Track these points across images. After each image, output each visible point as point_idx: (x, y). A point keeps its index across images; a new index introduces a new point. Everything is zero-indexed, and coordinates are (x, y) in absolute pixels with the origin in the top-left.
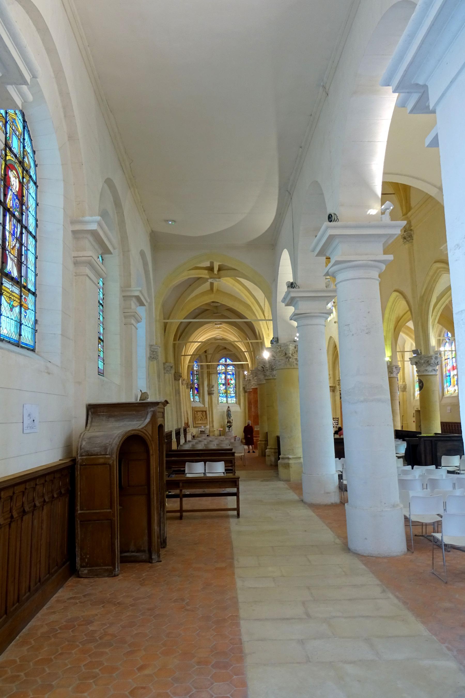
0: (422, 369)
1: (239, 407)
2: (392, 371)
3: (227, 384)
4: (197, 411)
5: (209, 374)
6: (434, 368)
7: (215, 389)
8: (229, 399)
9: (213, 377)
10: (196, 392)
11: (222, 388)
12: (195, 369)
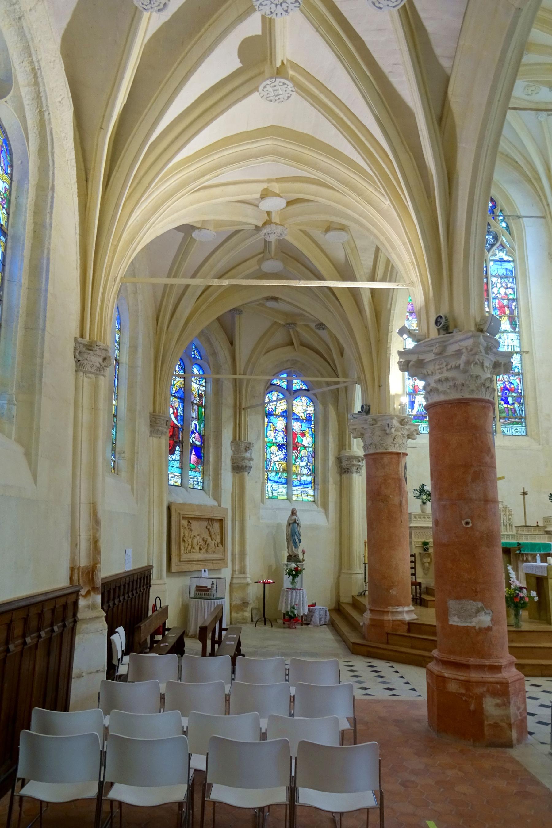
1: (325, 517)
3: (289, 445)
4: (190, 519)
5: (238, 411)
7: (255, 453)
8: (296, 491)
9: (251, 420)
10: (193, 457)
11: (277, 456)
12: (194, 386)
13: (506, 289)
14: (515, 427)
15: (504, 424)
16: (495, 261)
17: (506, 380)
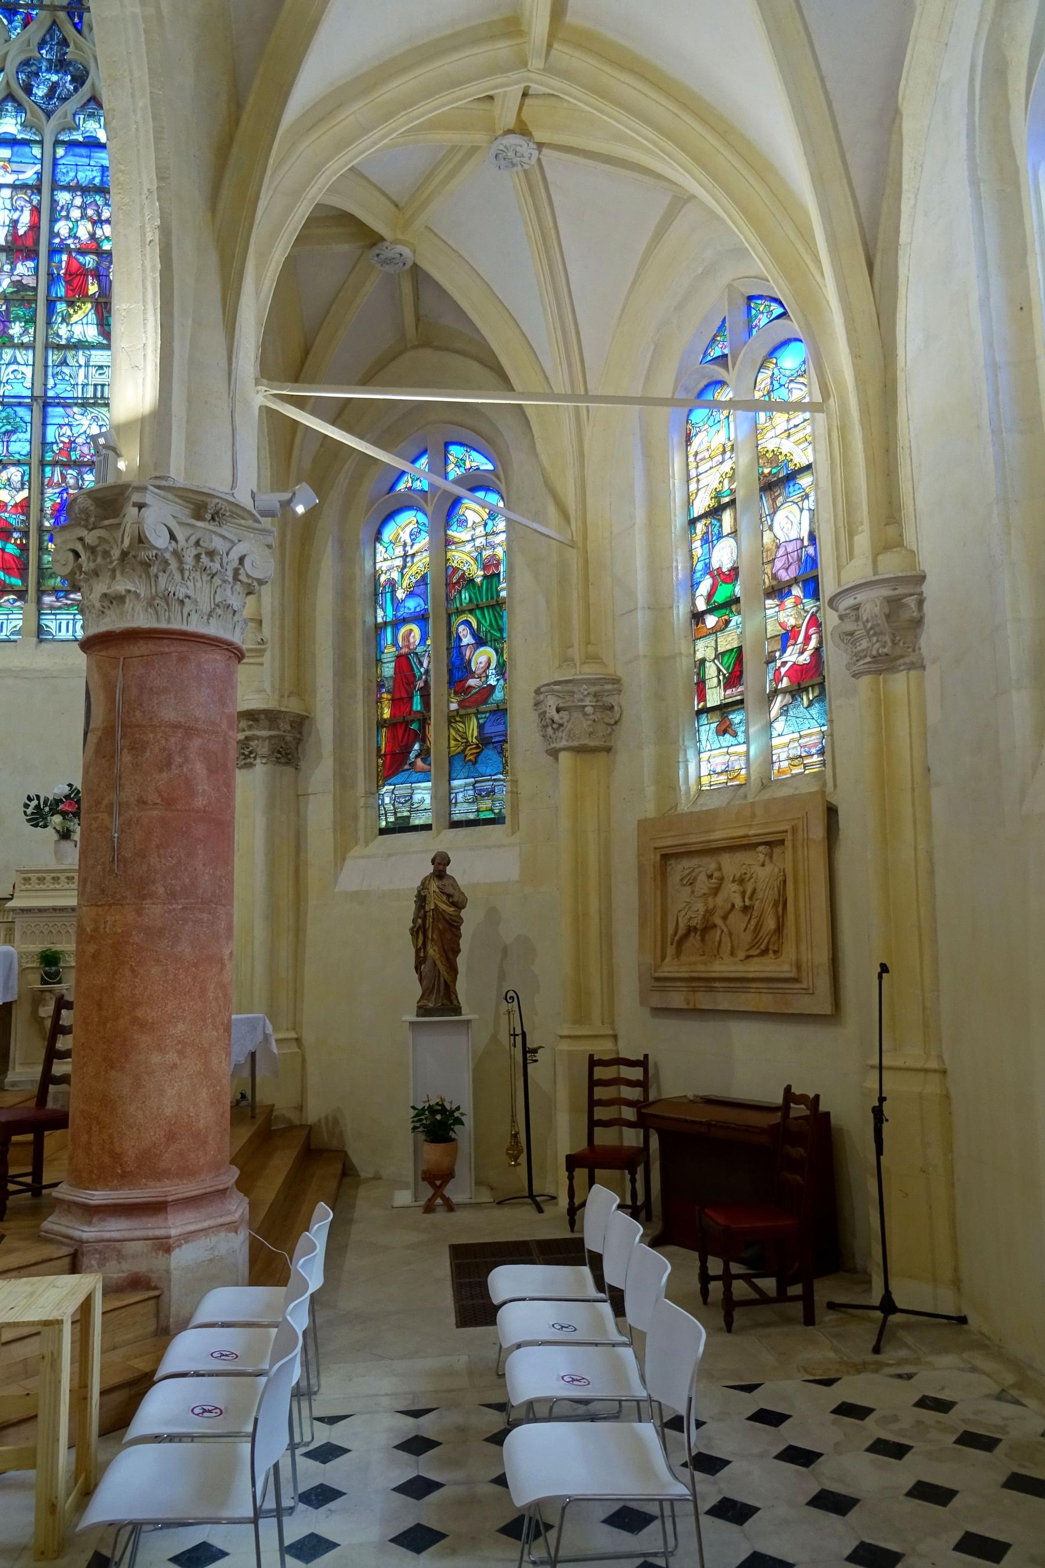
13: (94, 223)
15: (51, 608)
16: (72, 144)
17: (72, 482)
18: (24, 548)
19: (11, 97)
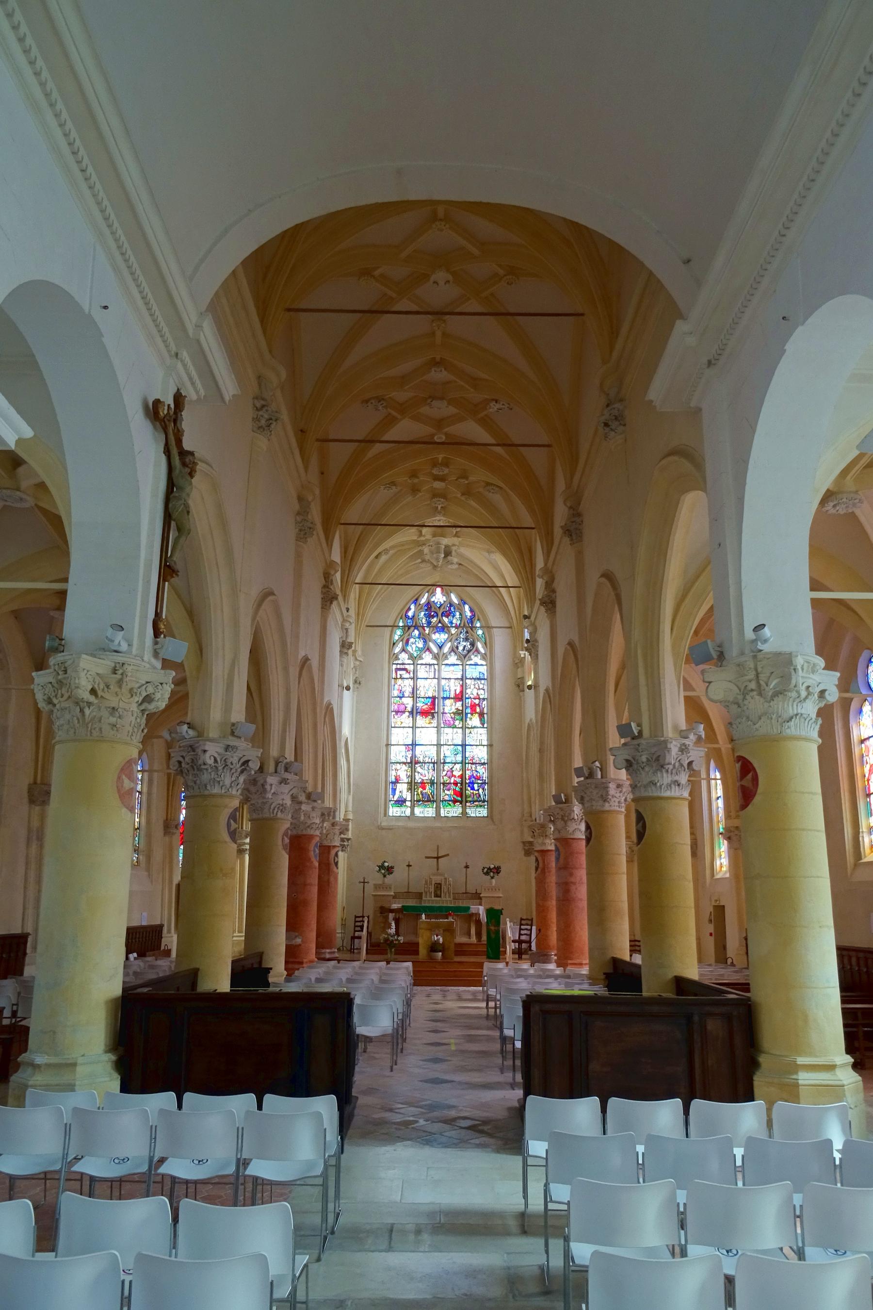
0: (645, 777)
2: (607, 794)
6: (676, 778)
14: (479, 809)
18: (461, 789)
19: (453, 650)
